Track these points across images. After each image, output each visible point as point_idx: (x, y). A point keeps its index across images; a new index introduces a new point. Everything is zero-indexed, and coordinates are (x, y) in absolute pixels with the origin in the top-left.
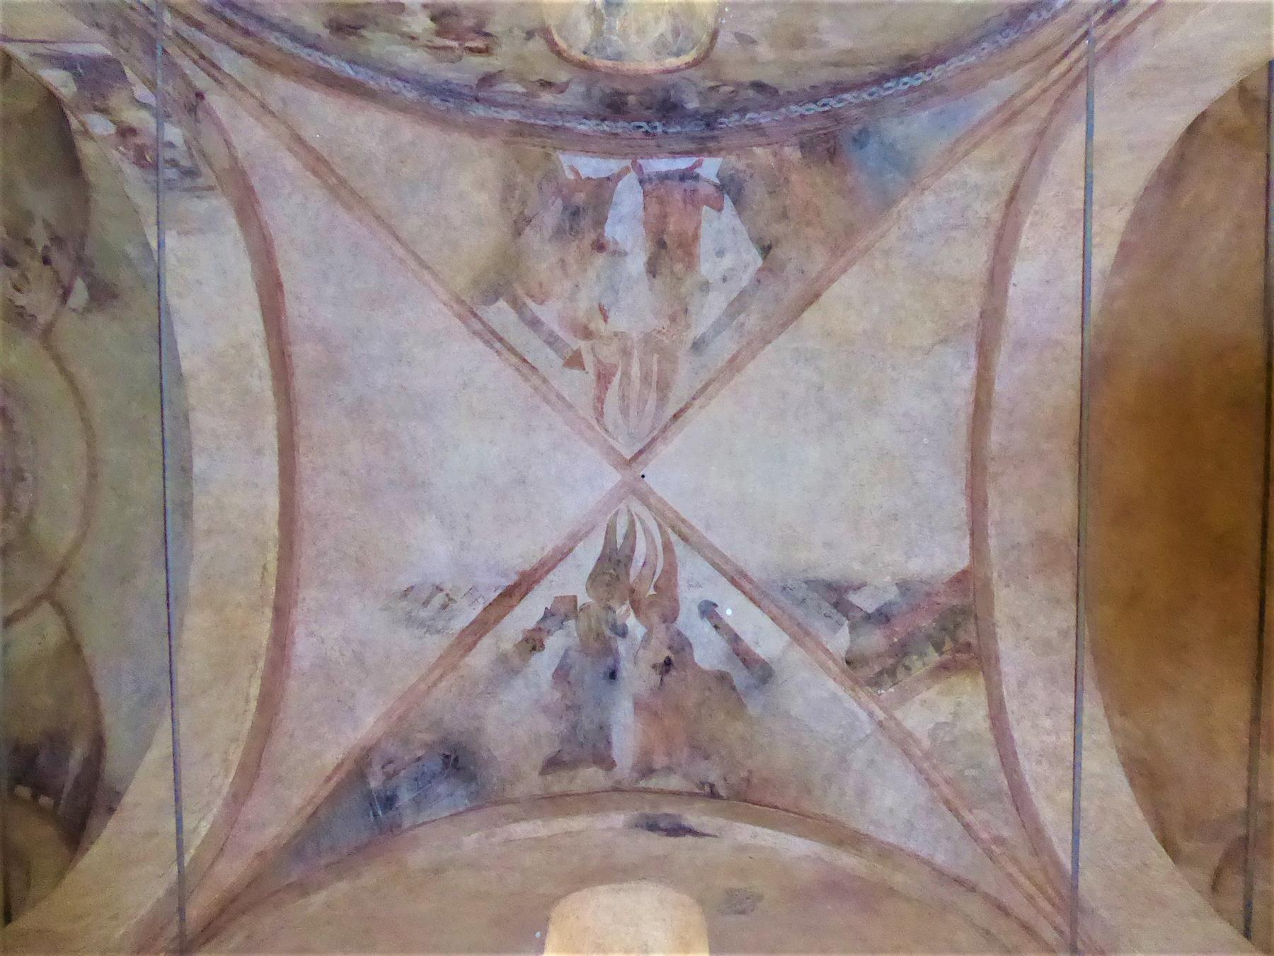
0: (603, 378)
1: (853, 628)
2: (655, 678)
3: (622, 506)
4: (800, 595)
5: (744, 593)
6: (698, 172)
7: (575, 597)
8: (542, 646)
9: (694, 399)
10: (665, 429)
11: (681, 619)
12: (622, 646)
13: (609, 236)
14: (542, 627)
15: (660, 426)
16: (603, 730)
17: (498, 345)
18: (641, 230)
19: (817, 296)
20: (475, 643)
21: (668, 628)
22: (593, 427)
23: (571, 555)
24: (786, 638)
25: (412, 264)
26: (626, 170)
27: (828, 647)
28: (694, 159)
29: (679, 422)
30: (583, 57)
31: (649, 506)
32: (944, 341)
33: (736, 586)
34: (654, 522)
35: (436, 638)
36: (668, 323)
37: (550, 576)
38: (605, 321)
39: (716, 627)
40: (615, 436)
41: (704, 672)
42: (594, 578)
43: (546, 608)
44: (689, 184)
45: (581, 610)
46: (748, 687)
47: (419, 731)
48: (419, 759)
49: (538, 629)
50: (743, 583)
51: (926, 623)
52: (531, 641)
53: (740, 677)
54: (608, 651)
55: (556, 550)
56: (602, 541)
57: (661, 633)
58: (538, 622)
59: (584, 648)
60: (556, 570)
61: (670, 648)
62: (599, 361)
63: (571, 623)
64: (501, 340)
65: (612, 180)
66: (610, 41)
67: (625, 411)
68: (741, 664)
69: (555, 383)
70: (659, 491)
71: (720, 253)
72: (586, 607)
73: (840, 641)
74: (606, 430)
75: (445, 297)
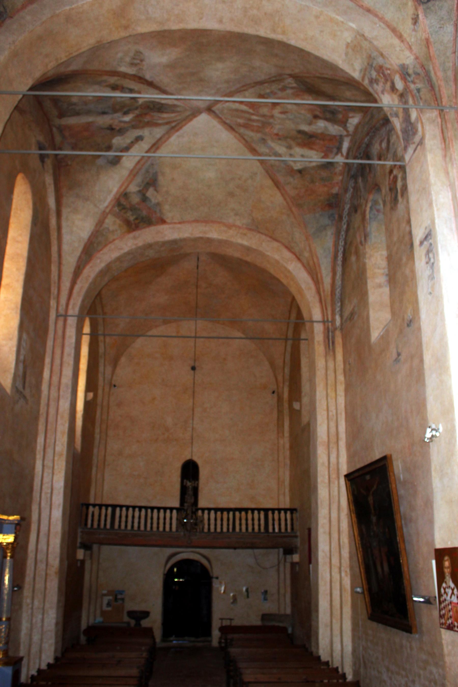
1: (140, 191)
19: (278, 187)
26: (347, 131)
32: (253, 220)
44: (335, 150)
51: (144, 213)
65: (345, 128)
73: (133, 188)
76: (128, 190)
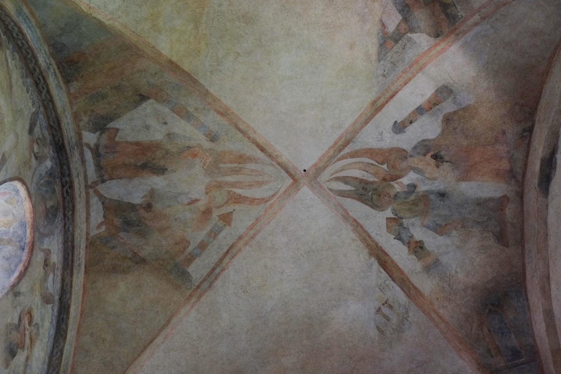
0: (239, 199)
2: (446, 165)
3: (325, 186)
4: (389, 65)
5: (387, 102)
6: (93, 145)
7: (387, 218)
8: (420, 242)
9: (249, 138)
10: (270, 156)
11: (404, 147)
12: (422, 188)
13: (141, 201)
14: (407, 241)
15: (268, 160)
16: (480, 203)
17: (217, 271)
18: (136, 181)
20: (415, 288)
21: (411, 156)
22: (271, 205)
23: (359, 221)
24: (419, 75)
25: (168, 330)
26: (97, 193)
27: (426, 48)
28: (85, 148)
29: (267, 148)
30: (26, 250)
31: (325, 167)
33: (382, 108)
34: (336, 164)
35: (411, 314)
36: (197, 159)
37: (373, 235)
38: (199, 200)
39: (411, 122)
40: (277, 190)
41: (443, 132)
42: (374, 206)
43: (394, 238)
44: (102, 151)
45: (396, 215)
46: (455, 103)
47: (471, 330)
48: (489, 331)
49: (408, 244)
50: (379, 103)
52: (416, 250)
53: (448, 107)
54: (425, 196)
55: (355, 231)
56: (349, 200)
57: (415, 161)
58: (404, 245)
59: (423, 214)
60: (369, 231)
61: (425, 155)
62: (227, 203)
63: (405, 222)
64: (214, 269)
66: (15, 232)
67: (260, 184)
68: (437, 107)
69: (242, 231)
70: (315, 160)
71: (147, 128)
72: (394, 211)
74: (273, 196)
75: (188, 308)
76: (432, 41)
